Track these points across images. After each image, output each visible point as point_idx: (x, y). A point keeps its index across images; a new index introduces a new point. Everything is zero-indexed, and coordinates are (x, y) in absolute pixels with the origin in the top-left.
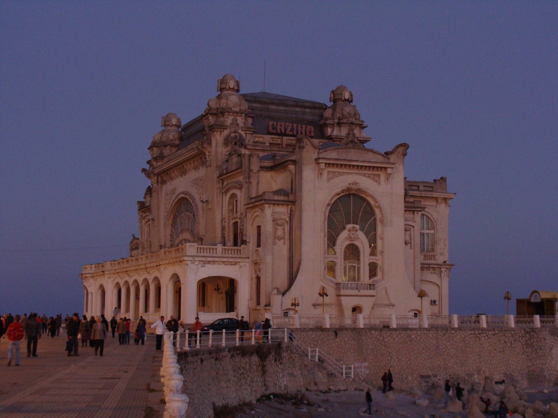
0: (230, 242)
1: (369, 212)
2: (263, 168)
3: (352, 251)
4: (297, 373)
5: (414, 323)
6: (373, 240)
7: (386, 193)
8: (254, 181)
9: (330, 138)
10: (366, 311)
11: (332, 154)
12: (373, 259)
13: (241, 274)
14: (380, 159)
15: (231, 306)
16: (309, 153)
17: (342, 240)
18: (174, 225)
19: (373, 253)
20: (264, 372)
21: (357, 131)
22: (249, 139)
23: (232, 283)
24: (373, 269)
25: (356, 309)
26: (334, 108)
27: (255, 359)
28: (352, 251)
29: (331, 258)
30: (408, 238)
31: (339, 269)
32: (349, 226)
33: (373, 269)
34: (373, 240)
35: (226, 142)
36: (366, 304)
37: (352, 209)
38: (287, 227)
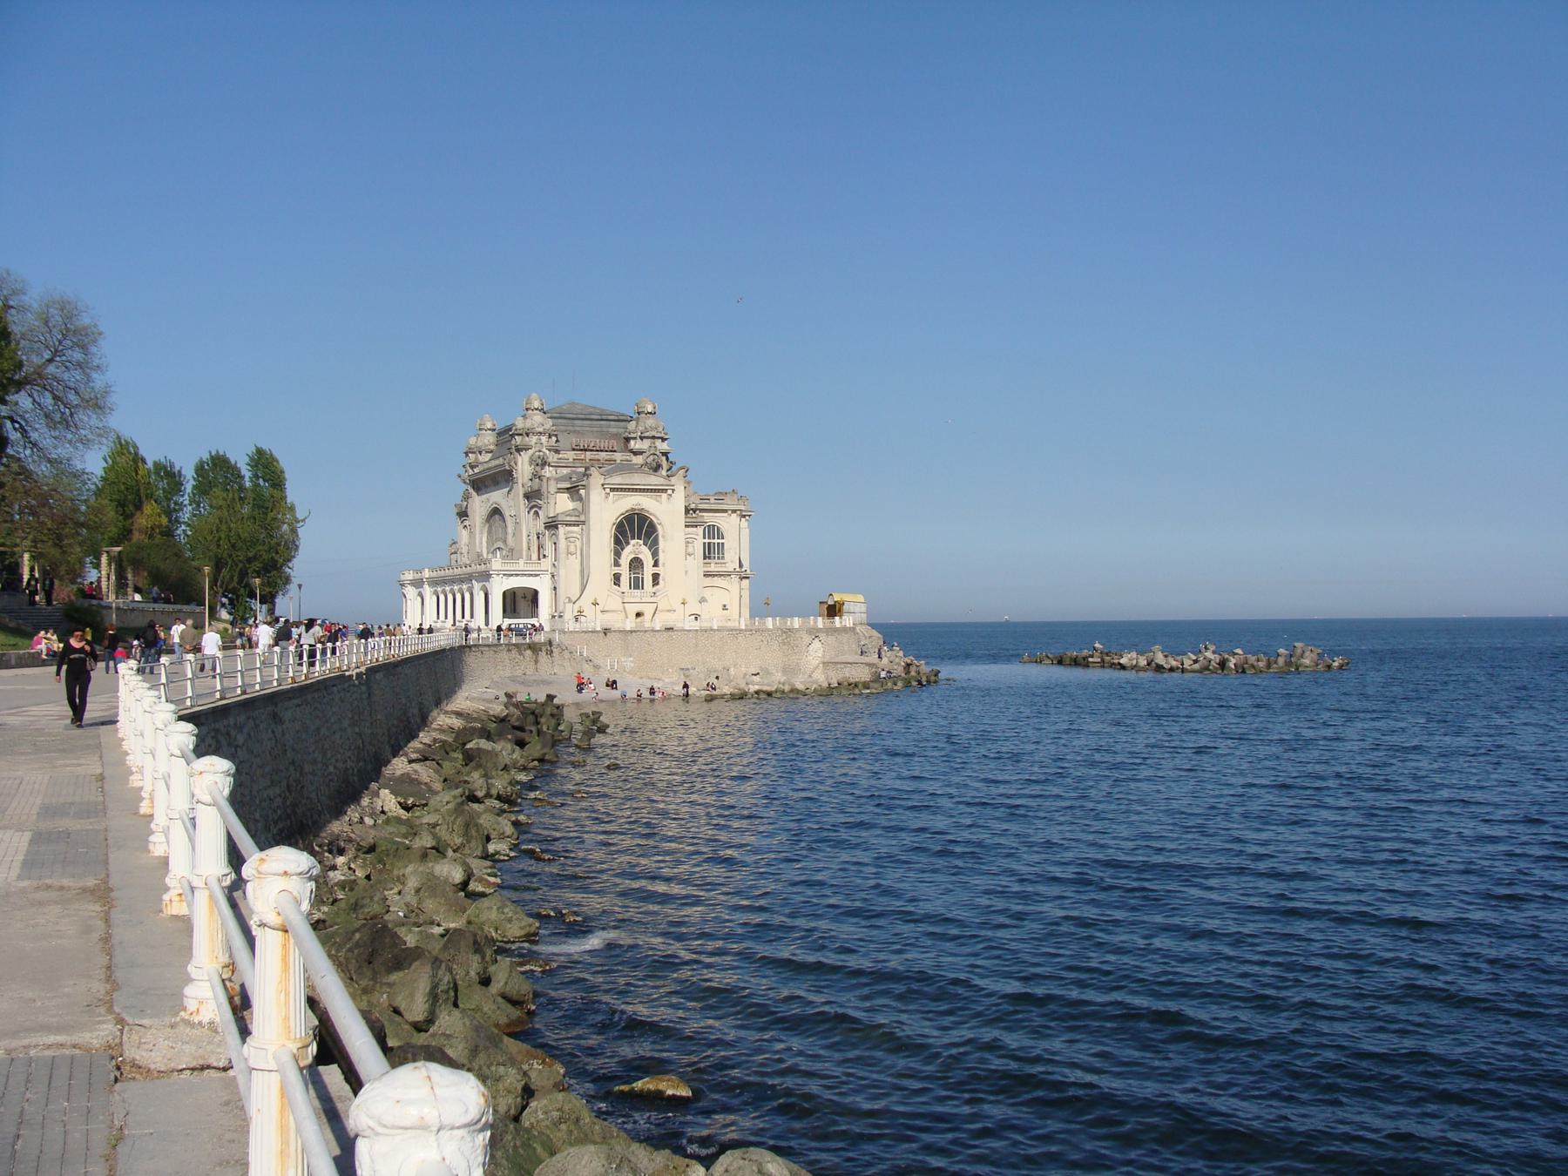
0: (535, 556)
1: (652, 529)
2: (560, 490)
3: (636, 564)
4: (567, 664)
5: (696, 625)
6: (655, 554)
7: (667, 511)
8: (552, 502)
9: (631, 451)
10: (648, 616)
11: (617, 480)
12: (656, 570)
13: (542, 586)
14: (661, 481)
15: (534, 614)
16: (596, 479)
17: (627, 554)
18: (490, 532)
19: (656, 564)
20: (536, 662)
21: (658, 443)
22: (552, 458)
23: (536, 592)
24: (656, 577)
25: (638, 615)
26: (637, 420)
27: (529, 652)
28: (636, 564)
29: (616, 570)
30: (690, 550)
31: (625, 580)
32: (632, 542)
33: (656, 577)
34: (655, 554)
35: (531, 461)
36: (648, 610)
37: (636, 527)
38: (578, 543)
